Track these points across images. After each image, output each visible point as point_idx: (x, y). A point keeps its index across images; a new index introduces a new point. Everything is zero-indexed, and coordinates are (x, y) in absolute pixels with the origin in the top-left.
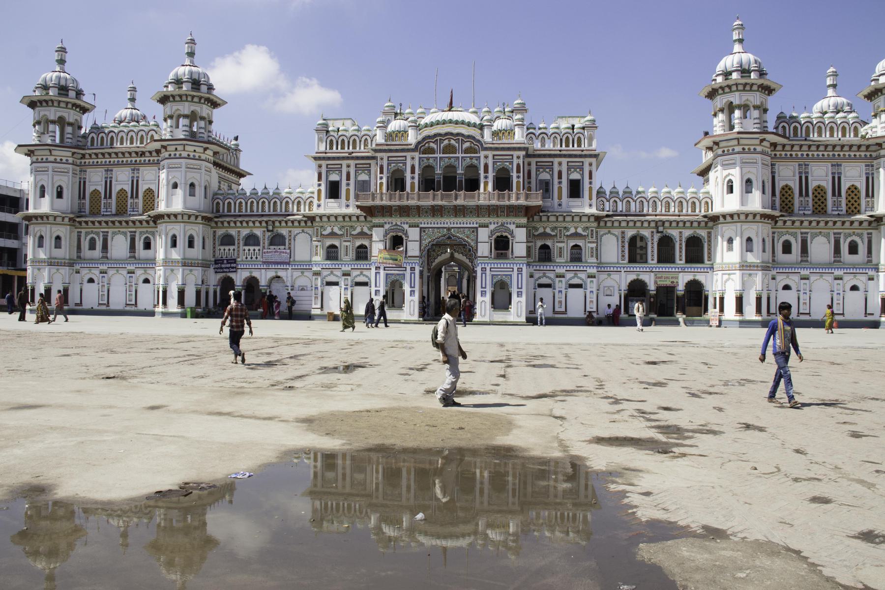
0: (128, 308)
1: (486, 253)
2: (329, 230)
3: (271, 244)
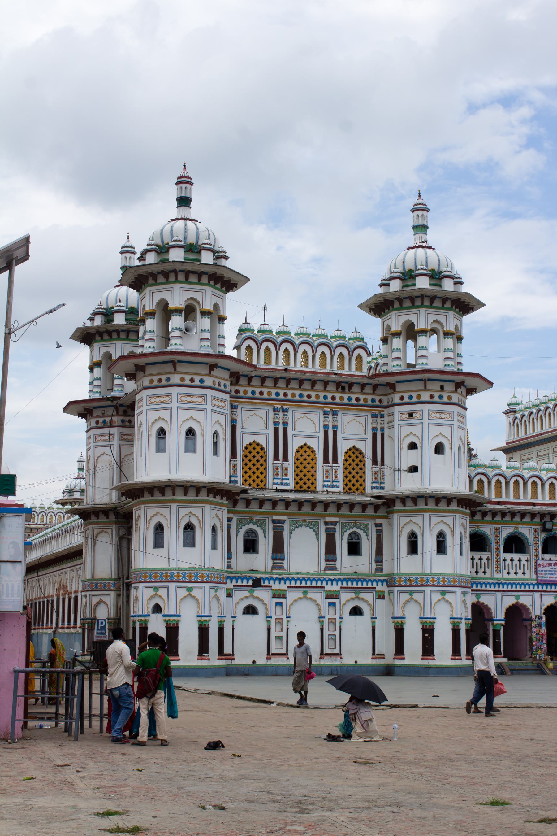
0: (327, 661)
3: (545, 551)
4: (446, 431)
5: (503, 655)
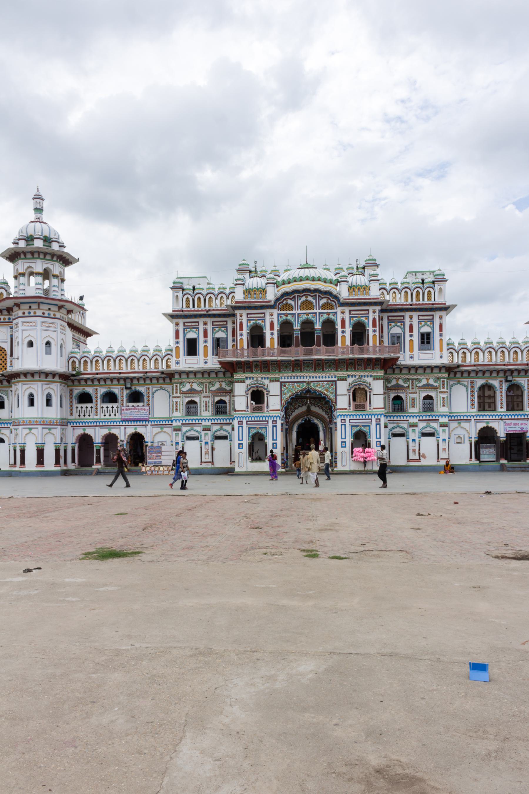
1: (346, 406)
2: (187, 387)
4: (33, 333)
5: (102, 463)
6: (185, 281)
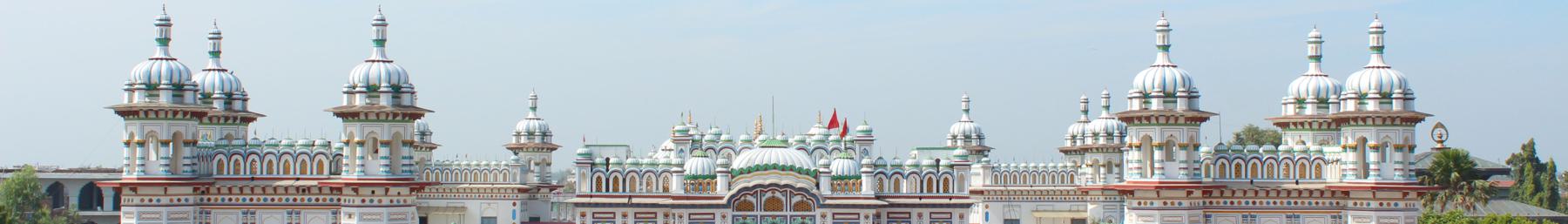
6: (595, 150)
